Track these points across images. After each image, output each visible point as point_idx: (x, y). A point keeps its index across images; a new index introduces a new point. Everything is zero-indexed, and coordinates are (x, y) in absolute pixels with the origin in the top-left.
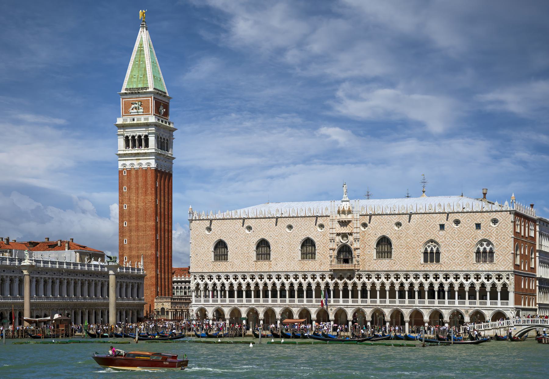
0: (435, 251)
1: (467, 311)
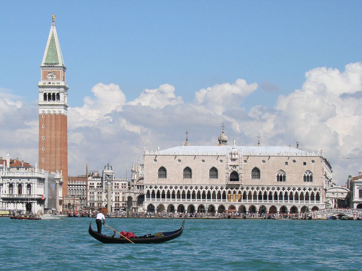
0: (283, 176)
1: (299, 206)
